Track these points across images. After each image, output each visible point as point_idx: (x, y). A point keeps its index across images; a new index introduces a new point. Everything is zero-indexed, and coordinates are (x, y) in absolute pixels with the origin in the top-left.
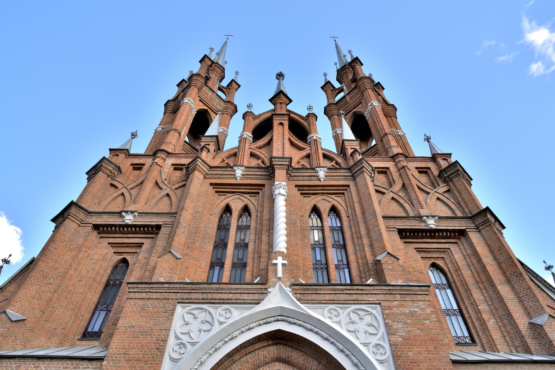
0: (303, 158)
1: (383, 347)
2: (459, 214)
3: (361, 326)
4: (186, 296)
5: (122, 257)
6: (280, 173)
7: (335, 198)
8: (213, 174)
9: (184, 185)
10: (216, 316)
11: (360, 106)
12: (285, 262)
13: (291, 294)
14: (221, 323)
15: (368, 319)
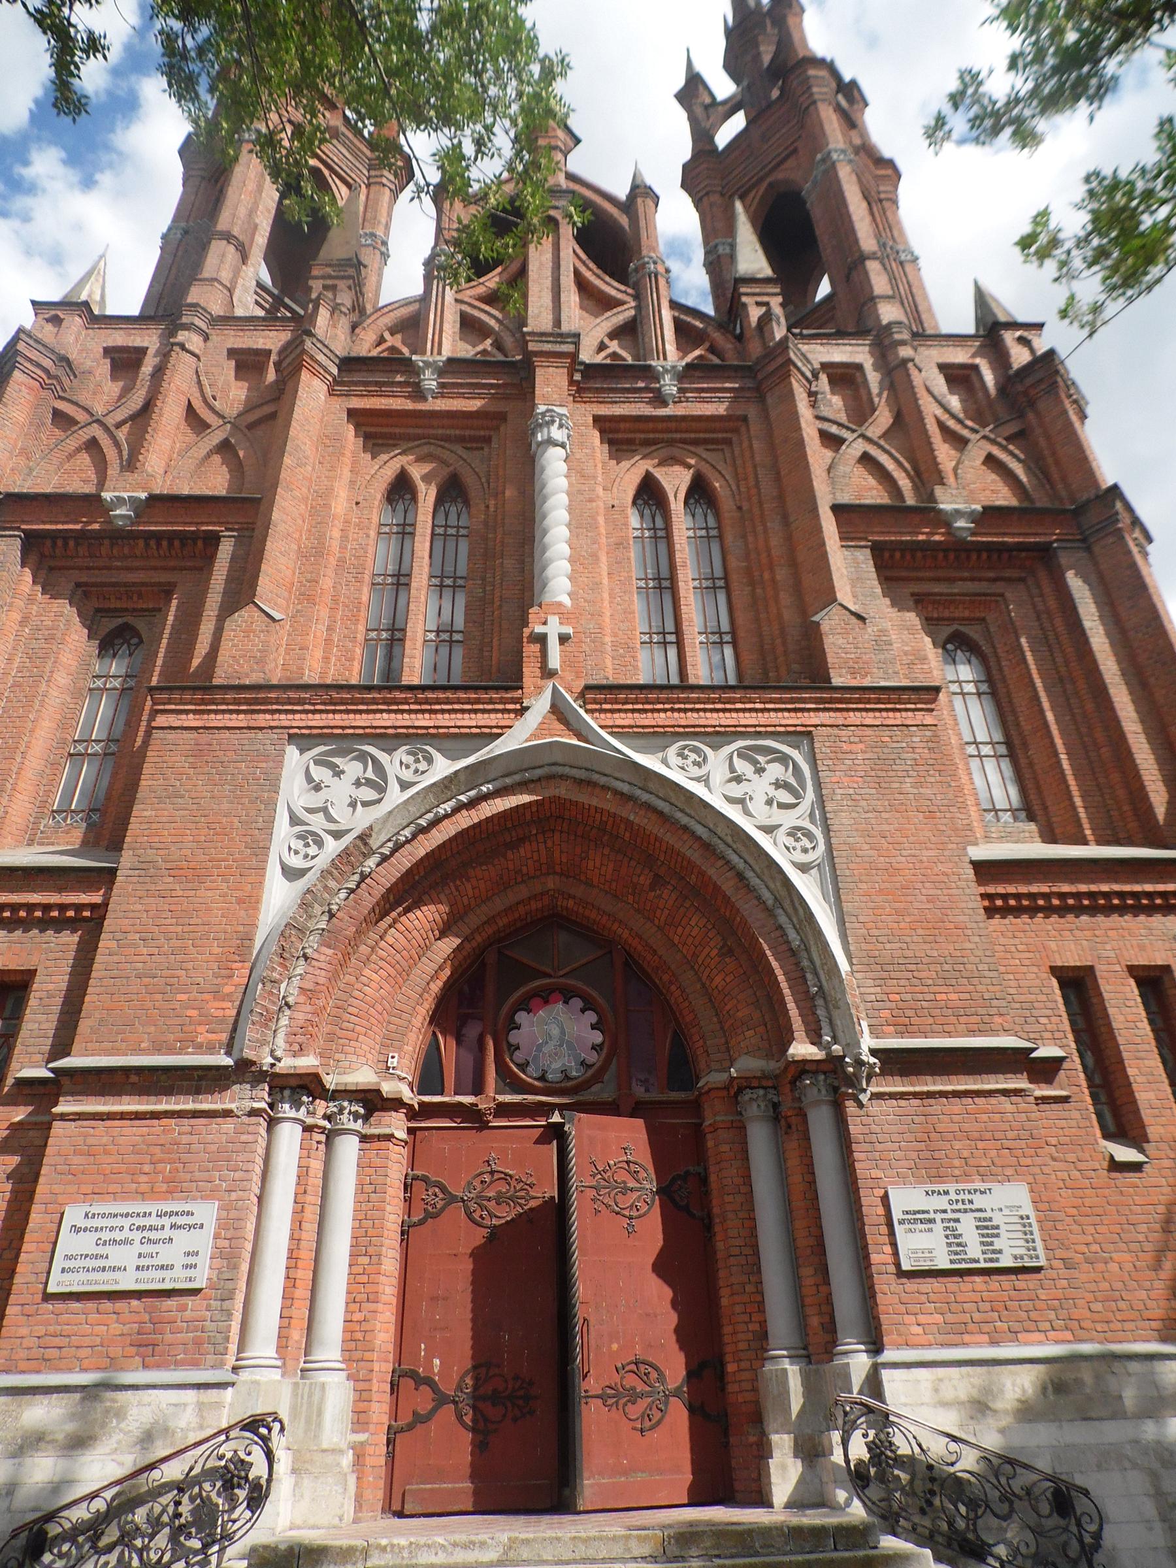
0: (612, 335)
1: (809, 835)
2: (1042, 502)
5: (120, 621)
6: (551, 384)
7: (705, 455)
9: (273, 416)
11: (791, 163)
12: (568, 630)
14: (404, 785)
15: (775, 770)
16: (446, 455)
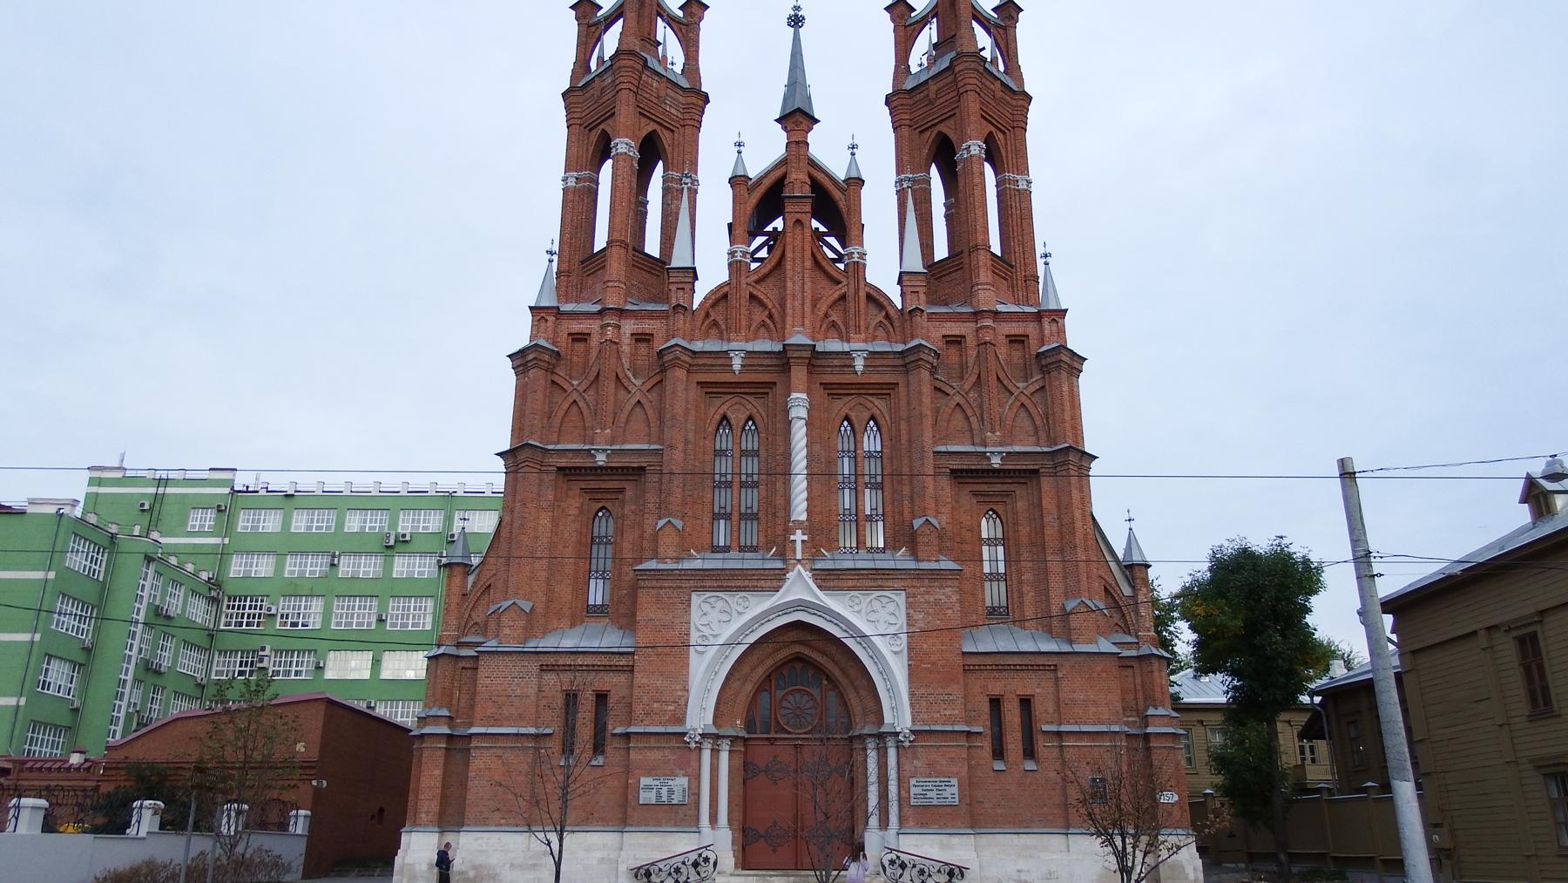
6: (799, 374)
10: (734, 606)
11: (951, 122)
13: (810, 582)
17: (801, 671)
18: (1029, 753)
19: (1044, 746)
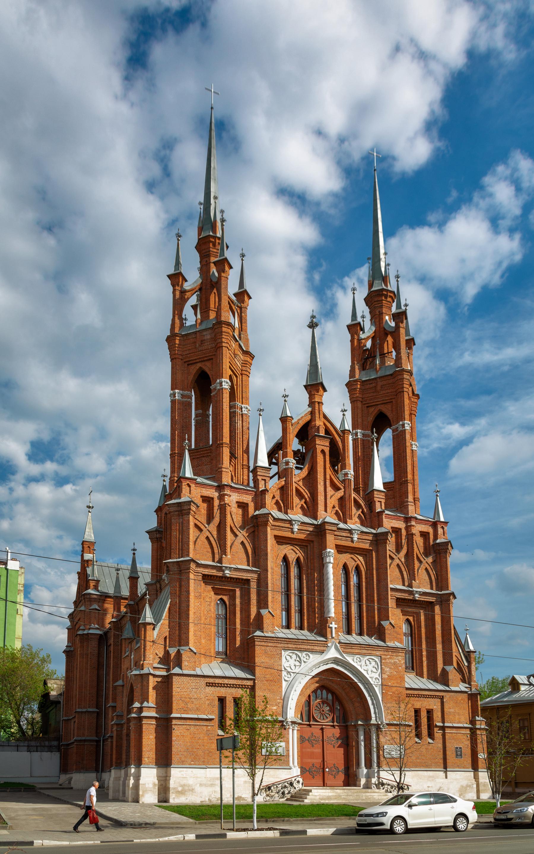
1: (379, 680)
3: (370, 667)
4: (286, 645)
8: (276, 526)
10: (302, 658)
12: (336, 626)
16: (298, 552)
17: (337, 694)
18: (431, 735)
19: (438, 734)
